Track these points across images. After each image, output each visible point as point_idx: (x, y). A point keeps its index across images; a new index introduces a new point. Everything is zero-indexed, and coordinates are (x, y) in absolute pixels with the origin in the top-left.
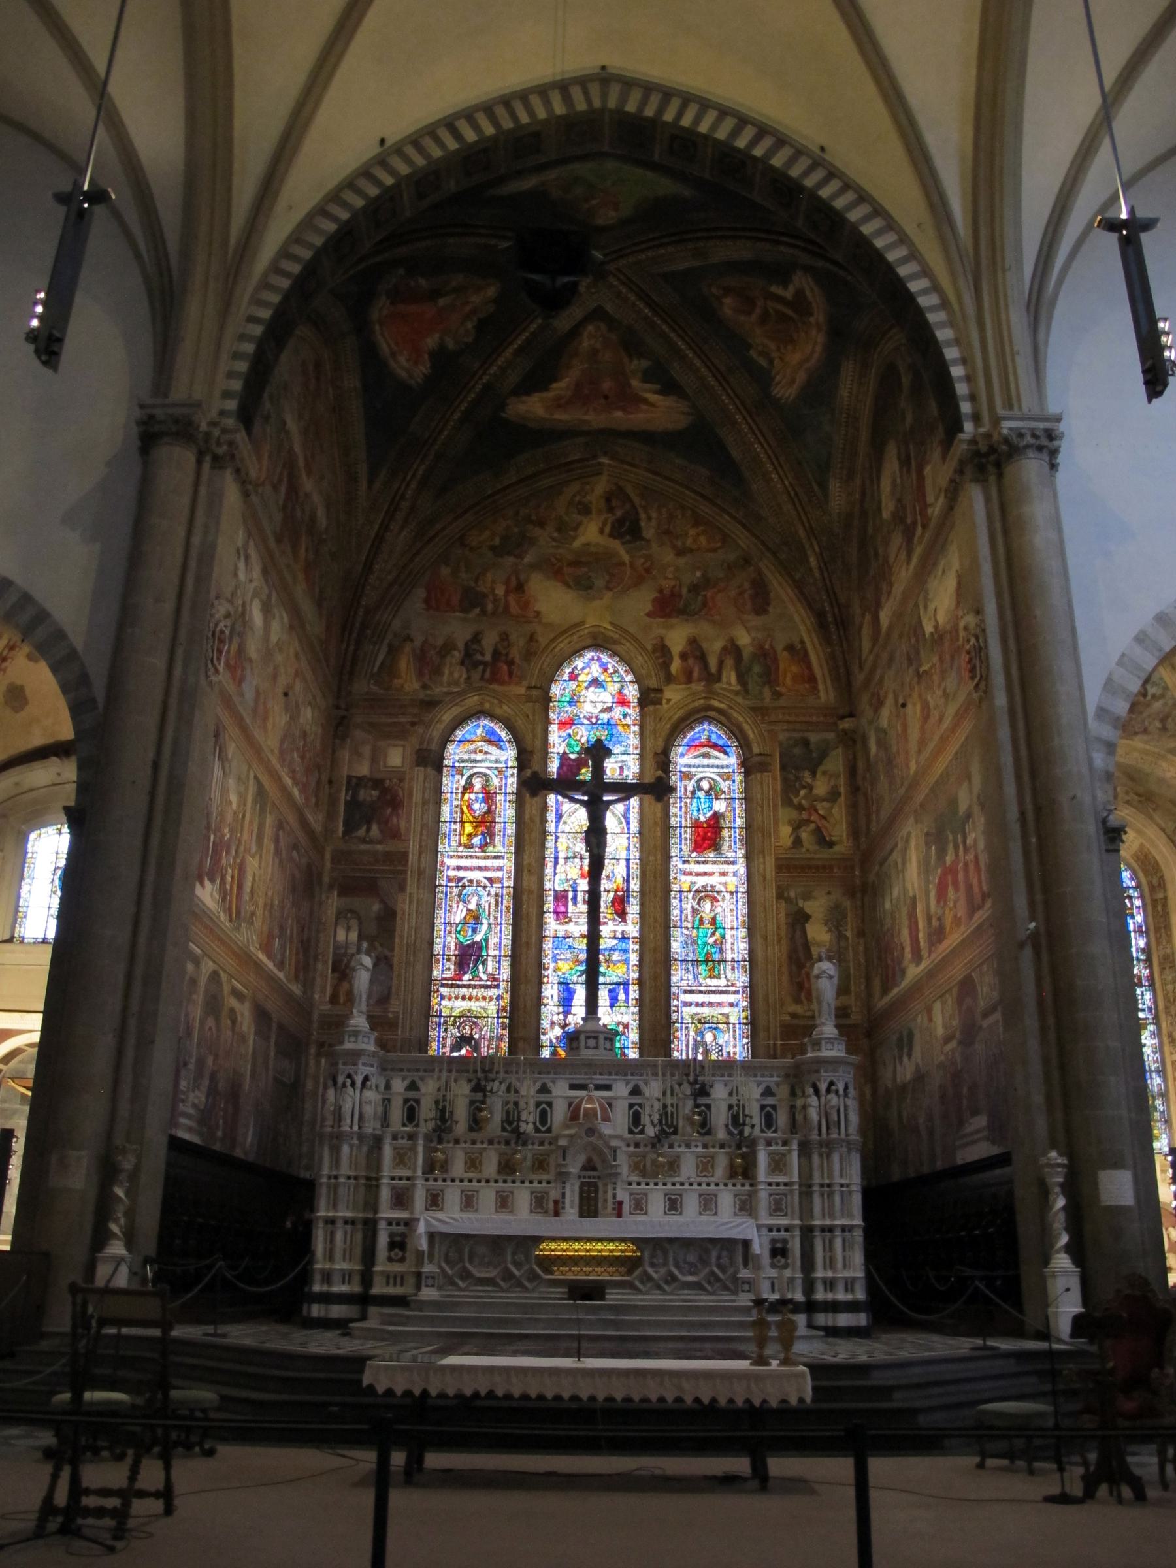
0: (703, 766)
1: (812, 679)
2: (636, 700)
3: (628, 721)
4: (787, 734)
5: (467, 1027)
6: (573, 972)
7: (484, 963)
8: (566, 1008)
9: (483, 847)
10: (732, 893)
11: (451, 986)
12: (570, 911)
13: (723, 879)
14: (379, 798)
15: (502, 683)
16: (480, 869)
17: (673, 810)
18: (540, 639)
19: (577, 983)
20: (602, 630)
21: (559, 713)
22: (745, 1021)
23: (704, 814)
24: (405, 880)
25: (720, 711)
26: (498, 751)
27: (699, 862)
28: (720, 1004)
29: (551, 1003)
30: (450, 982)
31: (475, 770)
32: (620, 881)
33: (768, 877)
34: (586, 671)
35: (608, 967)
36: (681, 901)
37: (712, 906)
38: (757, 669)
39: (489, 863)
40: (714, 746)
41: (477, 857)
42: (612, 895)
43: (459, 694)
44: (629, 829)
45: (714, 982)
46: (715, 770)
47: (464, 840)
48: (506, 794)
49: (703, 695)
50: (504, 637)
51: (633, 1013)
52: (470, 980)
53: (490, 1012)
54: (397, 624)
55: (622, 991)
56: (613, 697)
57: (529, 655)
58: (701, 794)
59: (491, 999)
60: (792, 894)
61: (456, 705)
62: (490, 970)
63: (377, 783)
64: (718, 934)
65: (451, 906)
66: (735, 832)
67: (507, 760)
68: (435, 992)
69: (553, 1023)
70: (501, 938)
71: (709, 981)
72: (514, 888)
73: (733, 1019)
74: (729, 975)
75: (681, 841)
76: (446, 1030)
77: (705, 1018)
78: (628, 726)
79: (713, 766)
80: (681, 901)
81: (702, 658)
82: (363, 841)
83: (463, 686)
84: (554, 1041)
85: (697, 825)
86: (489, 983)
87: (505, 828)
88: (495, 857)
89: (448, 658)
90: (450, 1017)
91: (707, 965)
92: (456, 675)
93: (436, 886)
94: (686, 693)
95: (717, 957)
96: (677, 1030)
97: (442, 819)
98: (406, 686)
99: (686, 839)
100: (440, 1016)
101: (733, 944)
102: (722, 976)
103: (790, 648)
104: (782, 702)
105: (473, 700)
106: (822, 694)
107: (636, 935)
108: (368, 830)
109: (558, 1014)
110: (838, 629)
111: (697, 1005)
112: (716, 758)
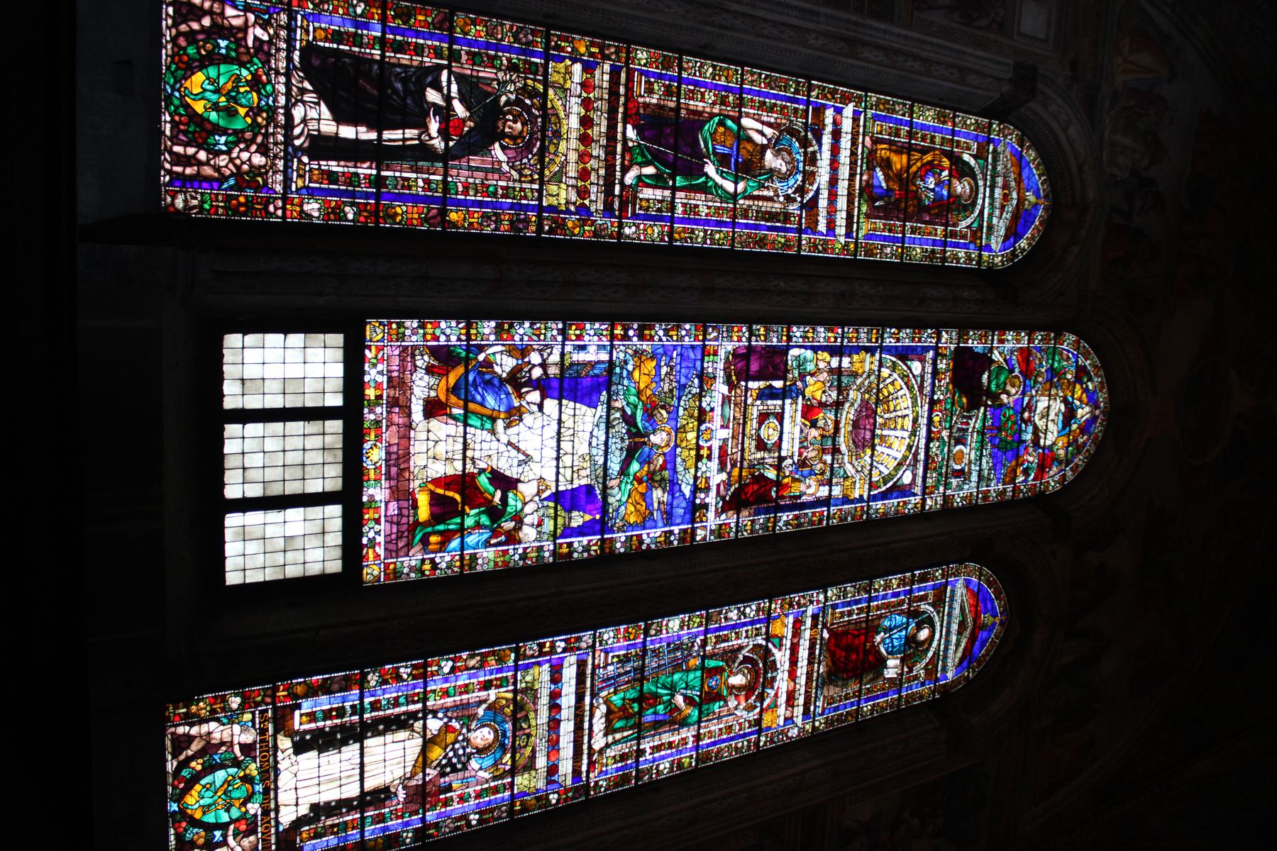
5: (519, 126)
6: (633, 399)
7: (658, 181)
8: (555, 384)
10: (758, 722)
11: (613, 92)
12: (751, 384)
13: (782, 699)
16: (833, 182)
19: (609, 408)
30: (622, 90)
31: (981, 183)
32: (797, 489)
35: (640, 481)
37: (740, 688)
39: (842, 203)
42: (771, 474)
45: (599, 724)
46: (942, 647)
47: (883, 150)
48: (945, 244)
51: (540, 549)
53: (553, 188)
55: (588, 517)
59: (583, 193)
62: (647, 193)
65: (771, 109)
66: (852, 704)
68: (602, 48)
69: (524, 351)
70: (706, 222)
72: (798, 256)
73: (522, 781)
74: (610, 753)
75: (849, 604)
76: (512, 68)
77: (526, 718)
78: (1013, 481)
80: (752, 623)
84: (481, 357)
86: (617, 191)
87: (894, 240)
90: (546, 83)
91: (633, 700)
93: (808, 79)
95: (649, 717)
96: (501, 660)
99: (850, 613)
100: (547, 57)
101: (670, 743)
111: (555, 695)
112: (958, 645)
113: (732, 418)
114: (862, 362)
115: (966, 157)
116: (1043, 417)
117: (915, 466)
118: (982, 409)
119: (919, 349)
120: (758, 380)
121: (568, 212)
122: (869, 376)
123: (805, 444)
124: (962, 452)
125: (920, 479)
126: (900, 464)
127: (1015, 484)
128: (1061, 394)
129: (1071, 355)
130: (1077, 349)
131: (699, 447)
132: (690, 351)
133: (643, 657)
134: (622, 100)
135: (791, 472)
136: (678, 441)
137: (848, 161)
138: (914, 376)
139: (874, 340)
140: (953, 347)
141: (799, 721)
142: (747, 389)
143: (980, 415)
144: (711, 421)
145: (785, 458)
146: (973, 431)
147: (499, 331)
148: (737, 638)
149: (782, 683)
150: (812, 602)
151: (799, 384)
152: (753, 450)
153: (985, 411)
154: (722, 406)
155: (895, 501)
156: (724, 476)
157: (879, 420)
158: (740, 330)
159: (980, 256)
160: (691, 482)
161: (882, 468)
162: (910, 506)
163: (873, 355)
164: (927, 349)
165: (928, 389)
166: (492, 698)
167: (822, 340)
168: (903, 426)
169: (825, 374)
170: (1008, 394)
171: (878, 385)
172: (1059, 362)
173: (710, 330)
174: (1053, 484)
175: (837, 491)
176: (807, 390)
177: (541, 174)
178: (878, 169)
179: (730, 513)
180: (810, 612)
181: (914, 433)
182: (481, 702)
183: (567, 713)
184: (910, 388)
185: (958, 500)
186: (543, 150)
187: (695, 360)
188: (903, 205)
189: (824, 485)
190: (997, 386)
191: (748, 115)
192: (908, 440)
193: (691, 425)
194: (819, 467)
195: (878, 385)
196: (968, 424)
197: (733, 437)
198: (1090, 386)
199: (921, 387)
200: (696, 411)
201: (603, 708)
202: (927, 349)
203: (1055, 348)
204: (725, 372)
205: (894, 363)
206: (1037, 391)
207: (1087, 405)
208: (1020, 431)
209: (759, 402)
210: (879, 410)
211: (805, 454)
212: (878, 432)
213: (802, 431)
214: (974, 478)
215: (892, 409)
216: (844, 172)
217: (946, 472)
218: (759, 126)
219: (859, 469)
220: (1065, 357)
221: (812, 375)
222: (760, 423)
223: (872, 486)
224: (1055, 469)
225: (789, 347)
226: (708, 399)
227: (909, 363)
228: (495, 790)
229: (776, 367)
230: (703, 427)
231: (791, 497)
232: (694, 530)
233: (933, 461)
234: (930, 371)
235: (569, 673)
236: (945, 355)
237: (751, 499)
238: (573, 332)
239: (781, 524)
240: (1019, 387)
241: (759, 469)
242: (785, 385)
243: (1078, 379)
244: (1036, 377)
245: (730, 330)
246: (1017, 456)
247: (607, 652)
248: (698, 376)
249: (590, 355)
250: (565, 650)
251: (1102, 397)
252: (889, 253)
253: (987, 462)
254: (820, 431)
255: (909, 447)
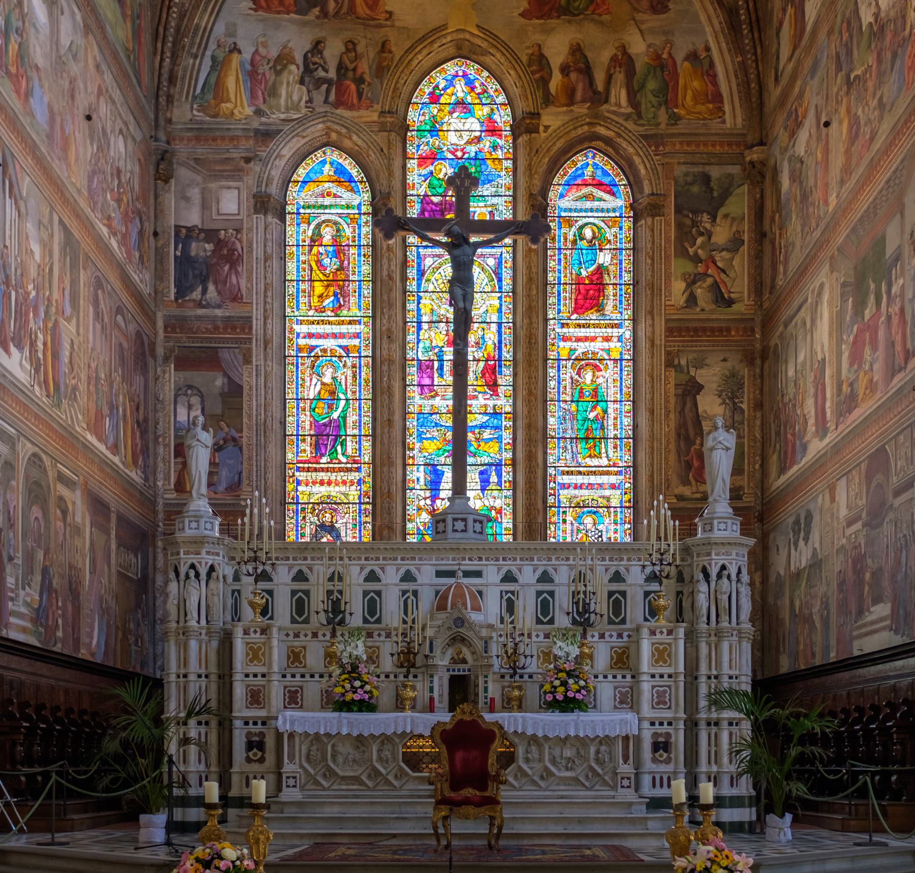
0: (586, 210)
1: (717, 98)
2: (508, 128)
3: (499, 154)
4: (684, 168)
5: (327, 515)
6: (441, 452)
8: (434, 493)
9: (336, 310)
10: (615, 360)
11: (308, 470)
12: (436, 383)
13: (606, 345)
14: (214, 251)
15: (351, 107)
16: (334, 336)
17: (551, 264)
18: (394, 49)
20: (468, 36)
21: (418, 146)
22: (627, 504)
23: (586, 268)
24: (250, 350)
25: (608, 141)
26: (349, 194)
27: (579, 326)
28: (601, 486)
29: (418, 487)
30: (306, 465)
31: (323, 218)
32: (490, 348)
33: (657, 342)
34: (449, 91)
35: (479, 446)
36: (559, 371)
38: (652, 85)
39: (344, 329)
40: (599, 185)
41: (330, 323)
42: (482, 364)
43: (300, 121)
44: (500, 288)
45: (595, 462)
46: (600, 214)
47: (315, 301)
49: (588, 120)
50: (351, 46)
51: (506, 497)
52: (328, 463)
53: (351, 498)
54: (220, 29)
55: (494, 473)
56: (482, 123)
57: (380, 70)
58: (583, 244)
59: (352, 483)
60: (683, 362)
61: (297, 135)
63: (211, 235)
64: (599, 409)
65: (303, 380)
66: (621, 290)
67: (360, 204)
69: (419, 509)
70: (360, 415)
71: (589, 461)
73: (615, 502)
74: (611, 454)
75: (559, 300)
76: (304, 518)
79: (597, 210)
80: (559, 371)
81: (587, 71)
82: (200, 305)
83: (304, 111)
84: (422, 528)
85: (579, 281)
86: (349, 466)
87: (360, 288)
88: (350, 323)
89: (285, 74)
91: (587, 443)
92: (295, 98)
93: (285, 357)
94: (567, 118)
95: (597, 434)
97: (288, 278)
98: (236, 112)
99: (565, 299)
100: (297, 503)
101: (615, 419)
102: (604, 455)
103: (693, 57)
104: (681, 128)
105: (317, 129)
106: (728, 116)
107: (508, 409)
108: (204, 291)
109: (425, 499)
110: (751, 31)
112: (601, 199)
115: (310, 233)
116: (461, 136)
121: (360, 490)
133: (565, 438)
134: (310, 465)
137: (322, 326)
141: (621, 331)
147: (410, 520)
148: (565, 380)
149: (598, 345)
150: (554, 329)
155: (504, 270)
159: (364, 214)
161: (484, 283)
166: (571, 519)
177: (345, 503)
178: (324, 304)
180: (558, 330)
182: (572, 524)
183: (585, 480)
186: (336, 503)
188: (341, 283)
191: (308, 395)
194: (480, 333)
201: (588, 460)
202: (418, 253)
216: (328, 329)
218: (312, 387)
225: (418, 360)
228: (616, 516)
235: (566, 479)
238: (411, 485)
247: (559, 459)
249: (421, 475)
250: (555, 482)
252: (367, 291)
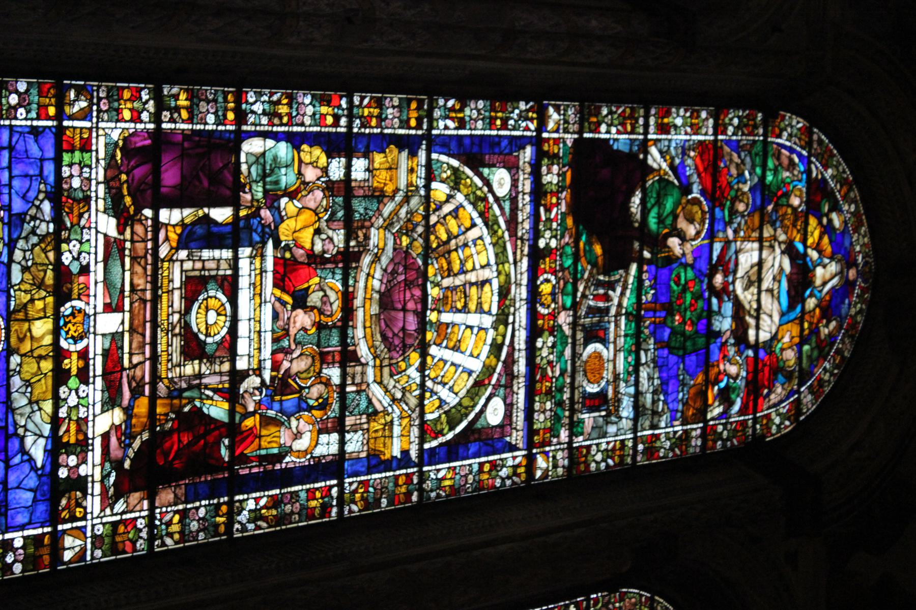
12: (164, 215)
42: (218, 410)
78: (701, 415)
113: (127, 288)
114: (392, 168)
117: (509, 386)
118: (634, 268)
119: (504, 143)
120: (181, 206)
122: (407, 199)
123: (285, 343)
124: (598, 356)
125: (521, 415)
126: (479, 384)
127: (705, 421)
128: (782, 237)
129: (796, 160)
130: (808, 145)
131: (59, 354)
132: (31, 140)
135: (259, 403)
136: (13, 340)
138: (497, 199)
139: (413, 123)
140: (570, 138)
142: (157, 225)
143: (631, 280)
144: (84, 294)
145: (244, 375)
146: (618, 314)
151: (266, 213)
152: (176, 358)
153: (640, 271)
154: (106, 260)
156: (117, 416)
157: (434, 292)
158: (136, 97)
160: (47, 429)
161: (444, 393)
162: (504, 472)
163: (413, 154)
164: (519, 143)
165: (527, 225)
167: (307, 120)
168: (480, 304)
169: (319, 194)
170: (683, 238)
171: (426, 217)
172: (775, 171)
173: (72, 94)
174: (777, 420)
175: (355, 444)
176: (283, 228)
179: (135, 497)
181: (502, 319)
184: (490, 224)
185: (599, 457)
187: (42, 160)
189: (328, 432)
190: (661, 220)
192: (491, 333)
193: (39, 305)
194: (316, 391)
195: (426, 217)
196: (607, 298)
197: (132, 330)
198: (837, 223)
199: (512, 223)
200: (50, 274)
203: (765, 143)
204: (109, 189)
205: (455, 171)
206: (736, 232)
207: (832, 258)
208: (709, 313)
209: (183, 254)
210: (431, 271)
211: (286, 364)
212: (432, 316)
213: (276, 316)
214: (627, 411)
215: (456, 267)
217: (572, 399)
219: (399, 395)
220: (785, 162)
221: (292, 195)
222: (189, 300)
223: (426, 431)
224: (779, 390)
225: (240, 137)
226: (74, 246)
227: (486, 171)
229: (215, 179)
230: (66, 309)
231: (262, 459)
232: (57, 538)
233: (544, 376)
234: (528, 189)
236: (556, 156)
237: (177, 464)
239: (244, 517)
240: (702, 222)
241: (191, 400)
242: (236, 215)
243: (813, 208)
244: (733, 204)
245: (114, 96)
246: (706, 364)
248: (48, 196)
251: (859, 243)
253: (650, 378)
254: (314, 316)
255: (496, 348)
